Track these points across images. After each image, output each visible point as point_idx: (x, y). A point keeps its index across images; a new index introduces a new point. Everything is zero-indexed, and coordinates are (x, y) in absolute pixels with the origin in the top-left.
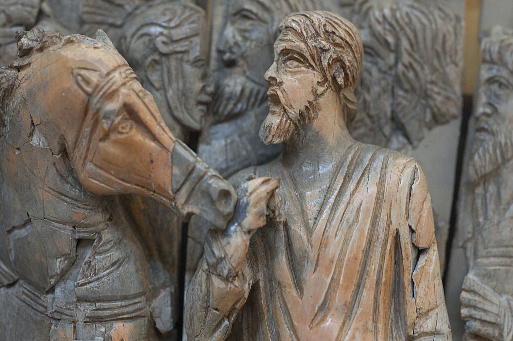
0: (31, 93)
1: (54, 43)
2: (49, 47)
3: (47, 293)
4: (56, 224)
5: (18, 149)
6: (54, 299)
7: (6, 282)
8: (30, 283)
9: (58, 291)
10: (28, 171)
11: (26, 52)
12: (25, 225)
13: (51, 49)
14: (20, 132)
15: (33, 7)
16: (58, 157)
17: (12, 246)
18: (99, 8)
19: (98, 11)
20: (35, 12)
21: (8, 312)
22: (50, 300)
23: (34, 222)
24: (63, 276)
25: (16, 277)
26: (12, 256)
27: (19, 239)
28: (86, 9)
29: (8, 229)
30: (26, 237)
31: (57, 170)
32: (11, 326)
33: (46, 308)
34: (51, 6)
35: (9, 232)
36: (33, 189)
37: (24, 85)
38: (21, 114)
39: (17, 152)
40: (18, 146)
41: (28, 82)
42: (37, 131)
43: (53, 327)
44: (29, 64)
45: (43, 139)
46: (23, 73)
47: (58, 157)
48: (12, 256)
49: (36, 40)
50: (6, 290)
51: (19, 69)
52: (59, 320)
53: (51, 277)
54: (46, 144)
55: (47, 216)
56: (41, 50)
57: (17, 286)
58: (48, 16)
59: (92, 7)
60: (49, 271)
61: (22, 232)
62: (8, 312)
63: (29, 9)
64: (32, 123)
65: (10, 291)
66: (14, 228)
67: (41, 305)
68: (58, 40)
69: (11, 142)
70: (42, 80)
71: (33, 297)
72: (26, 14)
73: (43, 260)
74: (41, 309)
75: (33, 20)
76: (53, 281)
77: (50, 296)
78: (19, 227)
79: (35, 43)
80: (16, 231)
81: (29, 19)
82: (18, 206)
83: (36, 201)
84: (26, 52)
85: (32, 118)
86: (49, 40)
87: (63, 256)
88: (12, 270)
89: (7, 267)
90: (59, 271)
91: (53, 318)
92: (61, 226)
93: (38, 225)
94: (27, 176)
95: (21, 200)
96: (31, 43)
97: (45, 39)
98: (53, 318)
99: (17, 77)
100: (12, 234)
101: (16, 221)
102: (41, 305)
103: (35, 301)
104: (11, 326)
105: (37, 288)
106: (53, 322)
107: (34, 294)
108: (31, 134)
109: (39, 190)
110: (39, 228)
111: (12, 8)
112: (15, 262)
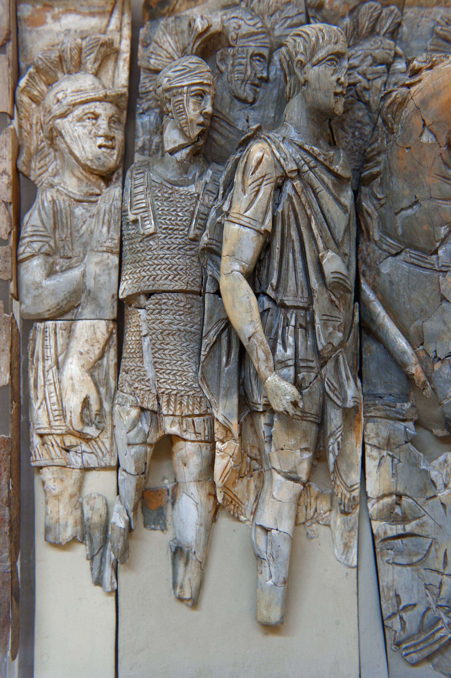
0: (424, 102)
1: (442, 61)
2: (438, 64)
3: (431, 255)
4: (440, 201)
5: (407, 148)
6: (438, 258)
7: (394, 252)
8: (416, 249)
9: (440, 252)
10: (416, 163)
11: (416, 72)
12: (410, 207)
13: (440, 65)
14: (411, 134)
15: (391, 50)
16: (445, 148)
17: (399, 224)
18: (440, 46)
19: (440, 49)
20: (392, 53)
21: (399, 272)
22: (435, 260)
23: (422, 203)
24: (443, 241)
25: (403, 247)
26: (400, 231)
27: (407, 217)
28: (432, 47)
29: (396, 211)
30: (414, 214)
31: (442, 159)
32: (403, 282)
33: (433, 265)
34: (402, 49)
35: (396, 214)
36: (421, 176)
37: (417, 96)
38: (413, 120)
39: (407, 151)
40: (408, 145)
41: (420, 93)
42: (426, 131)
43: (440, 277)
44: (420, 81)
45: (431, 136)
46: (413, 89)
47: (445, 148)
48: (400, 231)
49: (424, 62)
50: (394, 258)
51: (409, 86)
52: (446, 272)
53: (437, 242)
54: (434, 140)
55: (433, 196)
56: (431, 68)
57: (403, 253)
58: (400, 57)
59: (436, 45)
60: (436, 237)
61: (410, 212)
62: (399, 272)
63: (388, 51)
64: (424, 125)
65: (398, 258)
66: (402, 209)
67: (428, 263)
68: (445, 59)
69: (401, 144)
70: (435, 90)
71: (421, 259)
72: (386, 56)
73: (431, 229)
74: (429, 266)
75: (391, 60)
76: (438, 244)
77: (434, 257)
78: (406, 209)
79: (423, 65)
80: (403, 213)
81: (389, 59)
82: (407, 192)
83: (423, 186)
84: (416, 72)
85: (424, 120)
86: (439, 60)
87: (447, 224)
88: (399, 241)
89: (394, 241)
90: (443, 236)
91: (441, 271)
92: (445, 202)
93: (425, 204)
94: (416, 168)
95: (410, 187)
96: (420, 64)
97: (434, 59)
98: (441, 271)
99: (409, 92)
100: (399, 215)
101: (405, 203)
102: (428, 263)
103: (423, 262)
104: (403, 282)
105: (423, 251)
106: (441, 274)
107: (421, 257)
108: (421, 135)
109: (426, 176)
110: (426, 206)
111: (377, 51)
112: (403, 235)
